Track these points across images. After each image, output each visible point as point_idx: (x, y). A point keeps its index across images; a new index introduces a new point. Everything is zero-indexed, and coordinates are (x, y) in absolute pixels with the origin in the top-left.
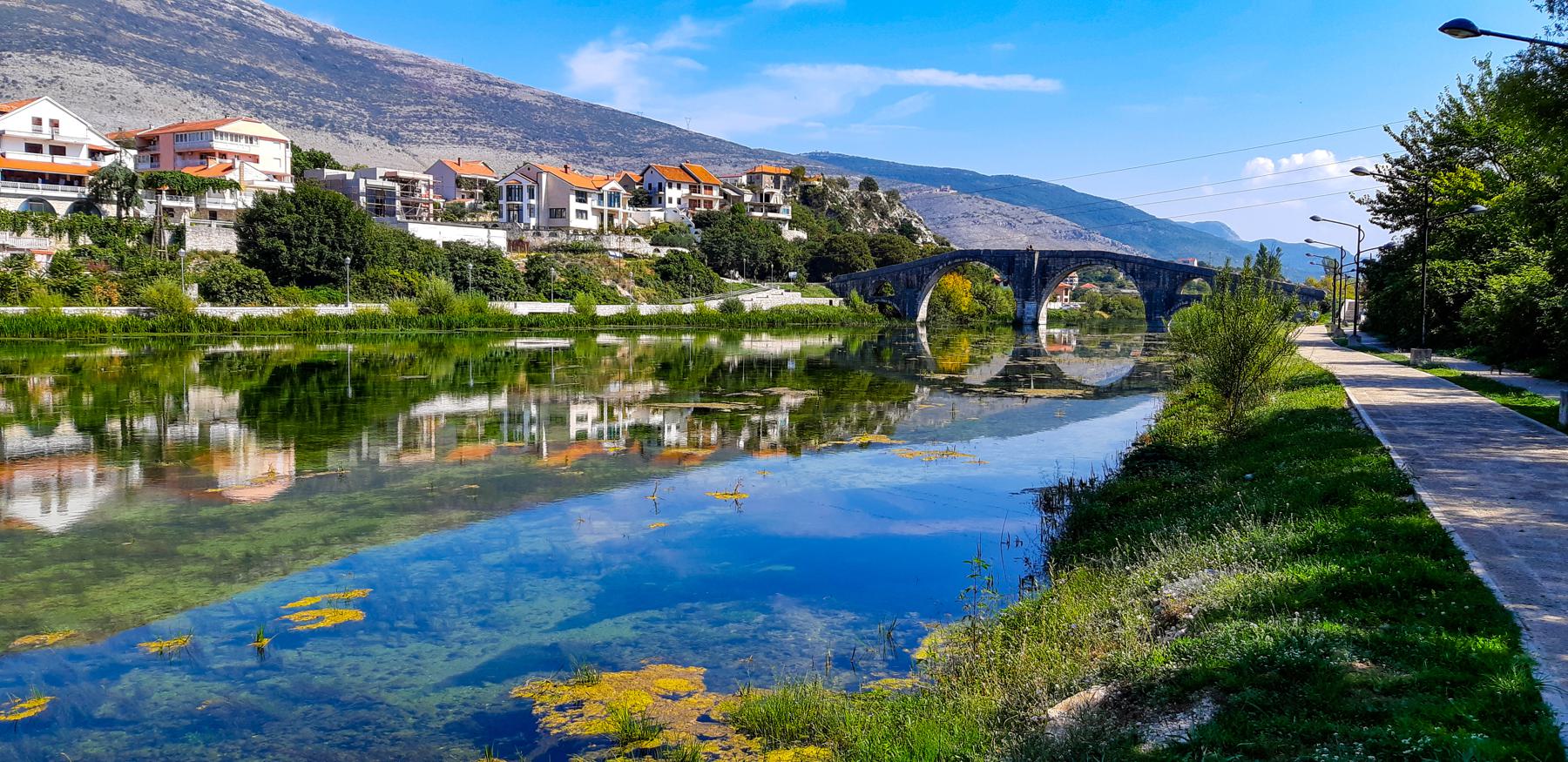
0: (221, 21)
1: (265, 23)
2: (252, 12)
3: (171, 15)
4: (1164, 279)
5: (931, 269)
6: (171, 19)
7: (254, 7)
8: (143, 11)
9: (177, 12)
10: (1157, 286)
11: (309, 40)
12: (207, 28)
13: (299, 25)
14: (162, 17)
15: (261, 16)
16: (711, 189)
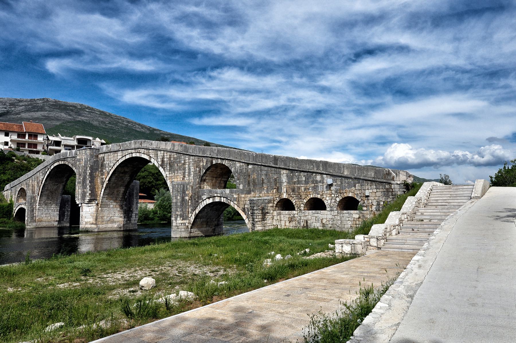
0: (122, 127)
1: (135, 127)
2: (132, 125)
3: (106, 125)
4: (189, 169)
5: (43, 174)
6: (106, 127)
7: (133, 123)
8: (98, 125)
9: (109, 125)
10: (184, 177)
11: (148, 132)
12: (117, 129)
13: (146, 128)
14: (104, 126)
15: (135, 125)
16: (36, 136)
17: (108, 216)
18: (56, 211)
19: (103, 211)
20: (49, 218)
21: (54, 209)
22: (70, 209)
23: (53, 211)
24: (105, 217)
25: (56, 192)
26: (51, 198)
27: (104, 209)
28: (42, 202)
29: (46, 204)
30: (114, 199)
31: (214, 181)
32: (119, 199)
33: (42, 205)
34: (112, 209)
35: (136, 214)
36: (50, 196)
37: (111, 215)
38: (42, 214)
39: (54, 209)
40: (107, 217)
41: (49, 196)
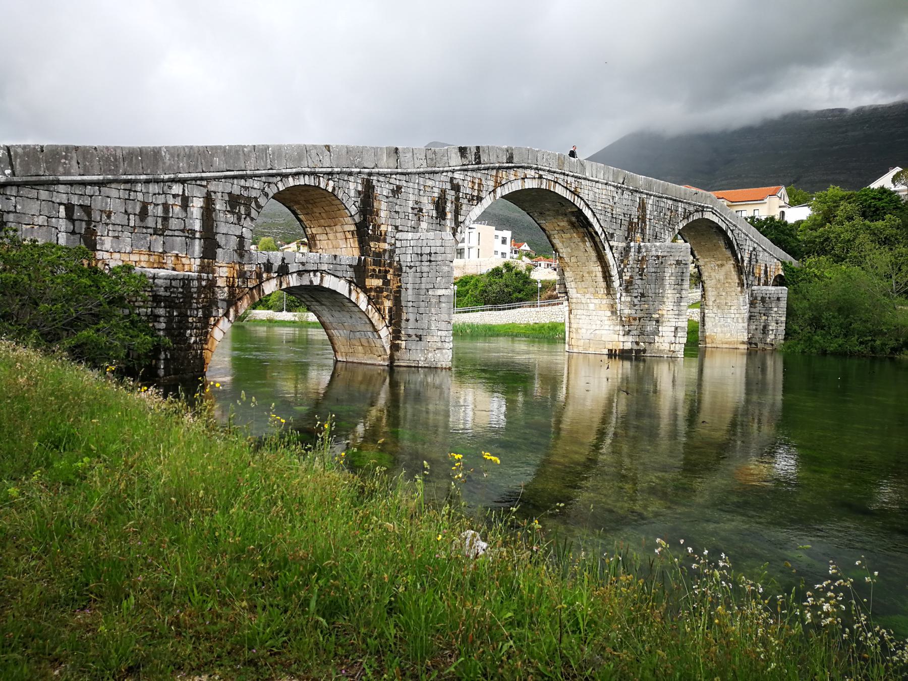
17: (589, 327)
18: (740, 320)
19: (578, 317)
20: (729, 334)
21: (737, 316)
22: (784, 319)
23: (735, 320)
24: (584, 331)
25: (730, 280)
26: (724, 294)
27: (580, 312)
28: (711, 303)
29: (718, 307)
30: (592, 290)
31: (331, 236)
32: (602, 289)
33: (711, 308)
34: (594, 313)
35: (676, 328)
36: (721, 289)
37: (594, 327)
38: (715, 326)
39: (737, 316)
40: (587, 330)
41: (719, 289)
